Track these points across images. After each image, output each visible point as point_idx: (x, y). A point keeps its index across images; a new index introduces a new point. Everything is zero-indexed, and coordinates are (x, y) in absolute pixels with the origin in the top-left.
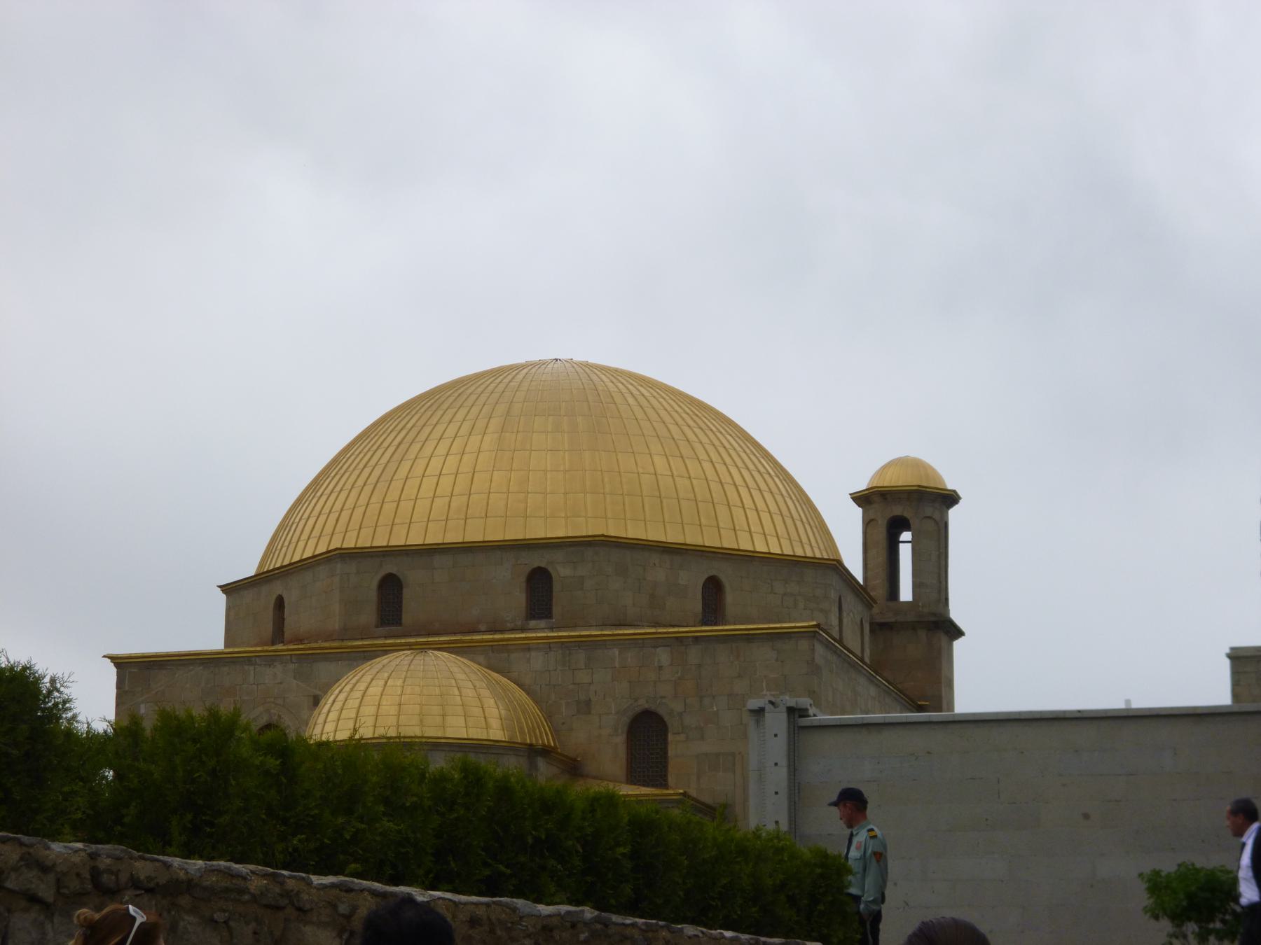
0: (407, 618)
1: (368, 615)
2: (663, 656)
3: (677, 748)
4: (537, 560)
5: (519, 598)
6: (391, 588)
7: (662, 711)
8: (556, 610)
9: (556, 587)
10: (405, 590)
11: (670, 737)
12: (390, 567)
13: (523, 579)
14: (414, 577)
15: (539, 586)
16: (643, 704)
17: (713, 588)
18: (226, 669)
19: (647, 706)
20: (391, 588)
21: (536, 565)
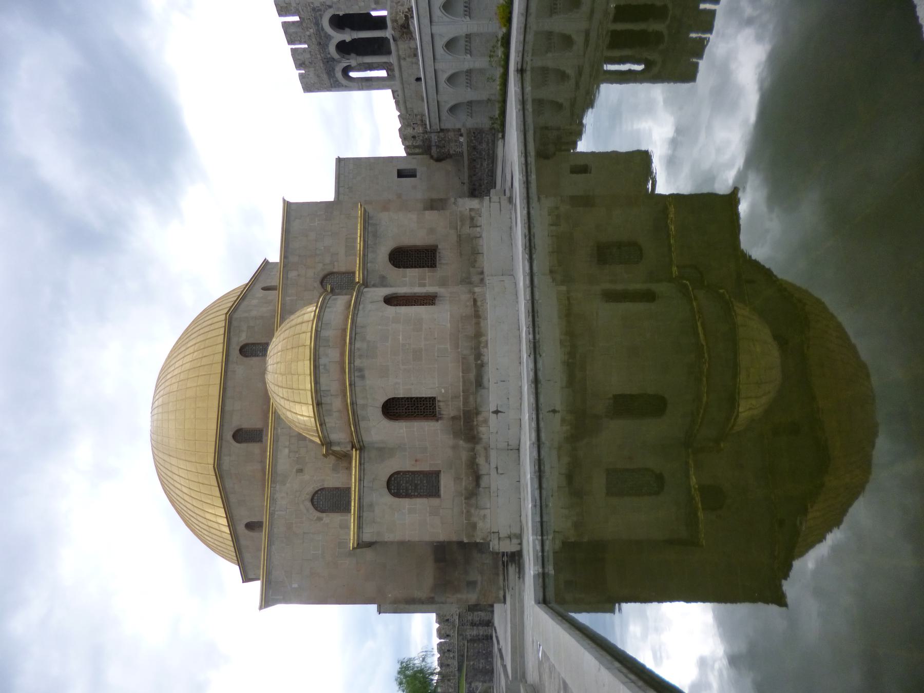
0: (259, 425)
1: (254, 448)
2: (292, 274)
3: (341, 267)
4: (235, 352)
6: (241, 436)
7: (322, 275)
8: (263, 341)
9: (251, 341)
10: (246, 425)
11: (335, 270)
12: (229, 436)
13: (245, 359)
14: (237, 422)
16: (317, 284)
17: (265, 289)
18: (275, 530)
19: (318, 282)
20: (241, 436)
21: (238, 352)
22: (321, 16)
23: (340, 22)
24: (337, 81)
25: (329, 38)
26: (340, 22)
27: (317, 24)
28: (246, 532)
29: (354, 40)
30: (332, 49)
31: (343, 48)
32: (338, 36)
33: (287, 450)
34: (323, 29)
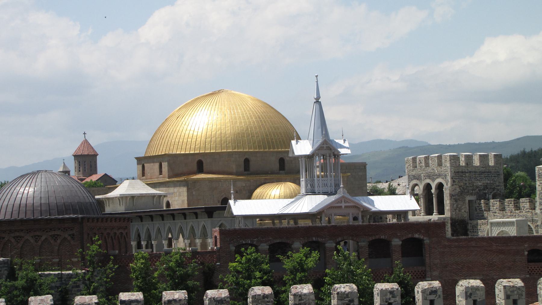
1: (242, 169)
5: (277, 166)
6: (247, 162)
9: (286, 162)
10: (251, 163)
12: (247, 157)
14: (252, 159)
15: (282, 161)
20: (247, 162)
22: (443, 178)
23: (440, 186)
24: (412, 180)
25: (433, 180)
26: (440, 186)
27: (439, 176)
28: (197, 160)
29: (432, 194)
30: (428, 181)
31: (428, 187)
32: (434, 186)
33: (244, 185)
34: (437, 178)
